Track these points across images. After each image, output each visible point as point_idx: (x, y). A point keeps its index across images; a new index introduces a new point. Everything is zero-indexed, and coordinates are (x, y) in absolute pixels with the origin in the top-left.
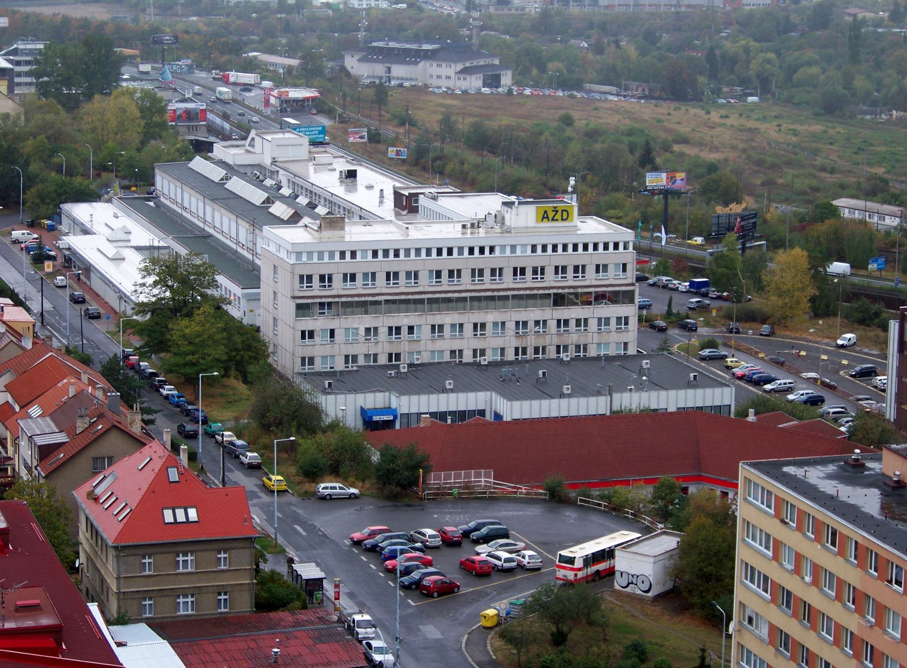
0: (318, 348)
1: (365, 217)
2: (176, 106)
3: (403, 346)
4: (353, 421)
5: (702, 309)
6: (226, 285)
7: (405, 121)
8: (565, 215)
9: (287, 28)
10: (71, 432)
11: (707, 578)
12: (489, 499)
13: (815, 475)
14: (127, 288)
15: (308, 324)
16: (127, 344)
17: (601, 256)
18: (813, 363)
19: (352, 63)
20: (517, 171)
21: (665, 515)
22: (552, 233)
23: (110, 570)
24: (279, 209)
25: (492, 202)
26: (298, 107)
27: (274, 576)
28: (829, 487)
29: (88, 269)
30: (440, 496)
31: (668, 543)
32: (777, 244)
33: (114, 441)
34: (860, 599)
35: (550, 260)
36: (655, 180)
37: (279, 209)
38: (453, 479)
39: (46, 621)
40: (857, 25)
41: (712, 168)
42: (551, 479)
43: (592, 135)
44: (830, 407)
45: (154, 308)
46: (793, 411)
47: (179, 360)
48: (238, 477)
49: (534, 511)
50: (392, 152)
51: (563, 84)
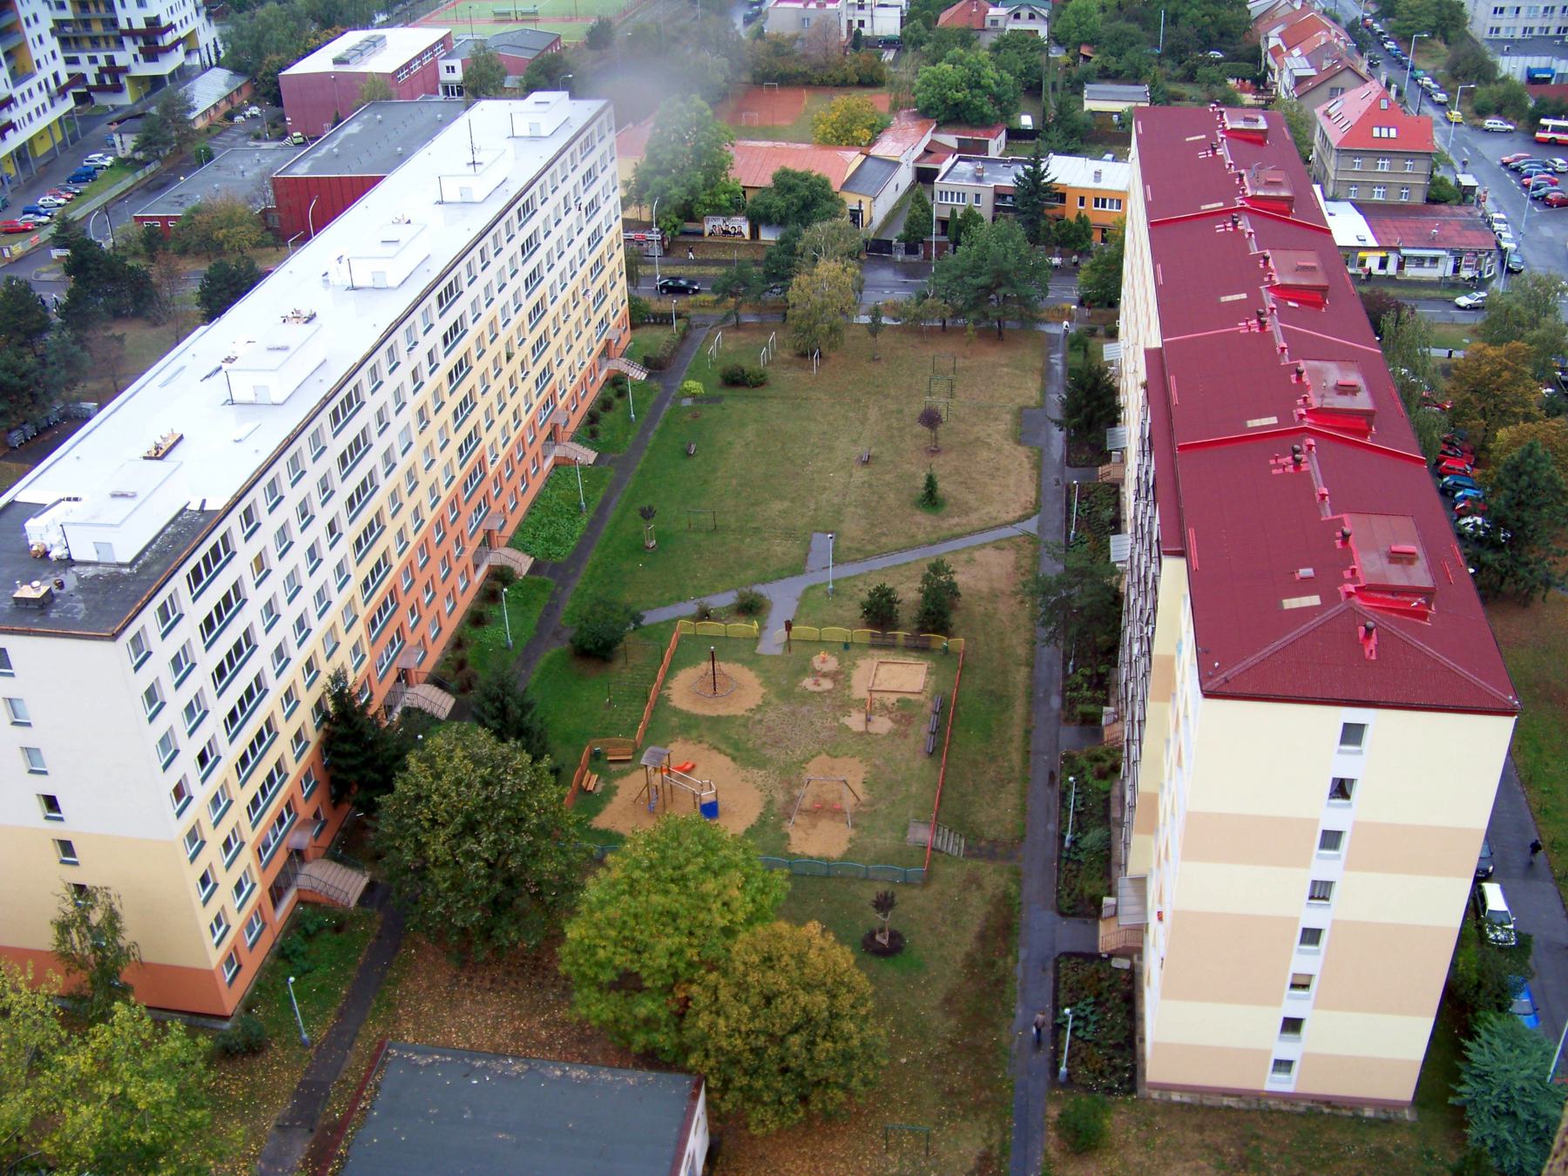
10: (1318, 69)
23: (1331, 164)
27: (1442, 182)
33: (1347, 78)
39: (1284, 193)
48: (1429, 110)
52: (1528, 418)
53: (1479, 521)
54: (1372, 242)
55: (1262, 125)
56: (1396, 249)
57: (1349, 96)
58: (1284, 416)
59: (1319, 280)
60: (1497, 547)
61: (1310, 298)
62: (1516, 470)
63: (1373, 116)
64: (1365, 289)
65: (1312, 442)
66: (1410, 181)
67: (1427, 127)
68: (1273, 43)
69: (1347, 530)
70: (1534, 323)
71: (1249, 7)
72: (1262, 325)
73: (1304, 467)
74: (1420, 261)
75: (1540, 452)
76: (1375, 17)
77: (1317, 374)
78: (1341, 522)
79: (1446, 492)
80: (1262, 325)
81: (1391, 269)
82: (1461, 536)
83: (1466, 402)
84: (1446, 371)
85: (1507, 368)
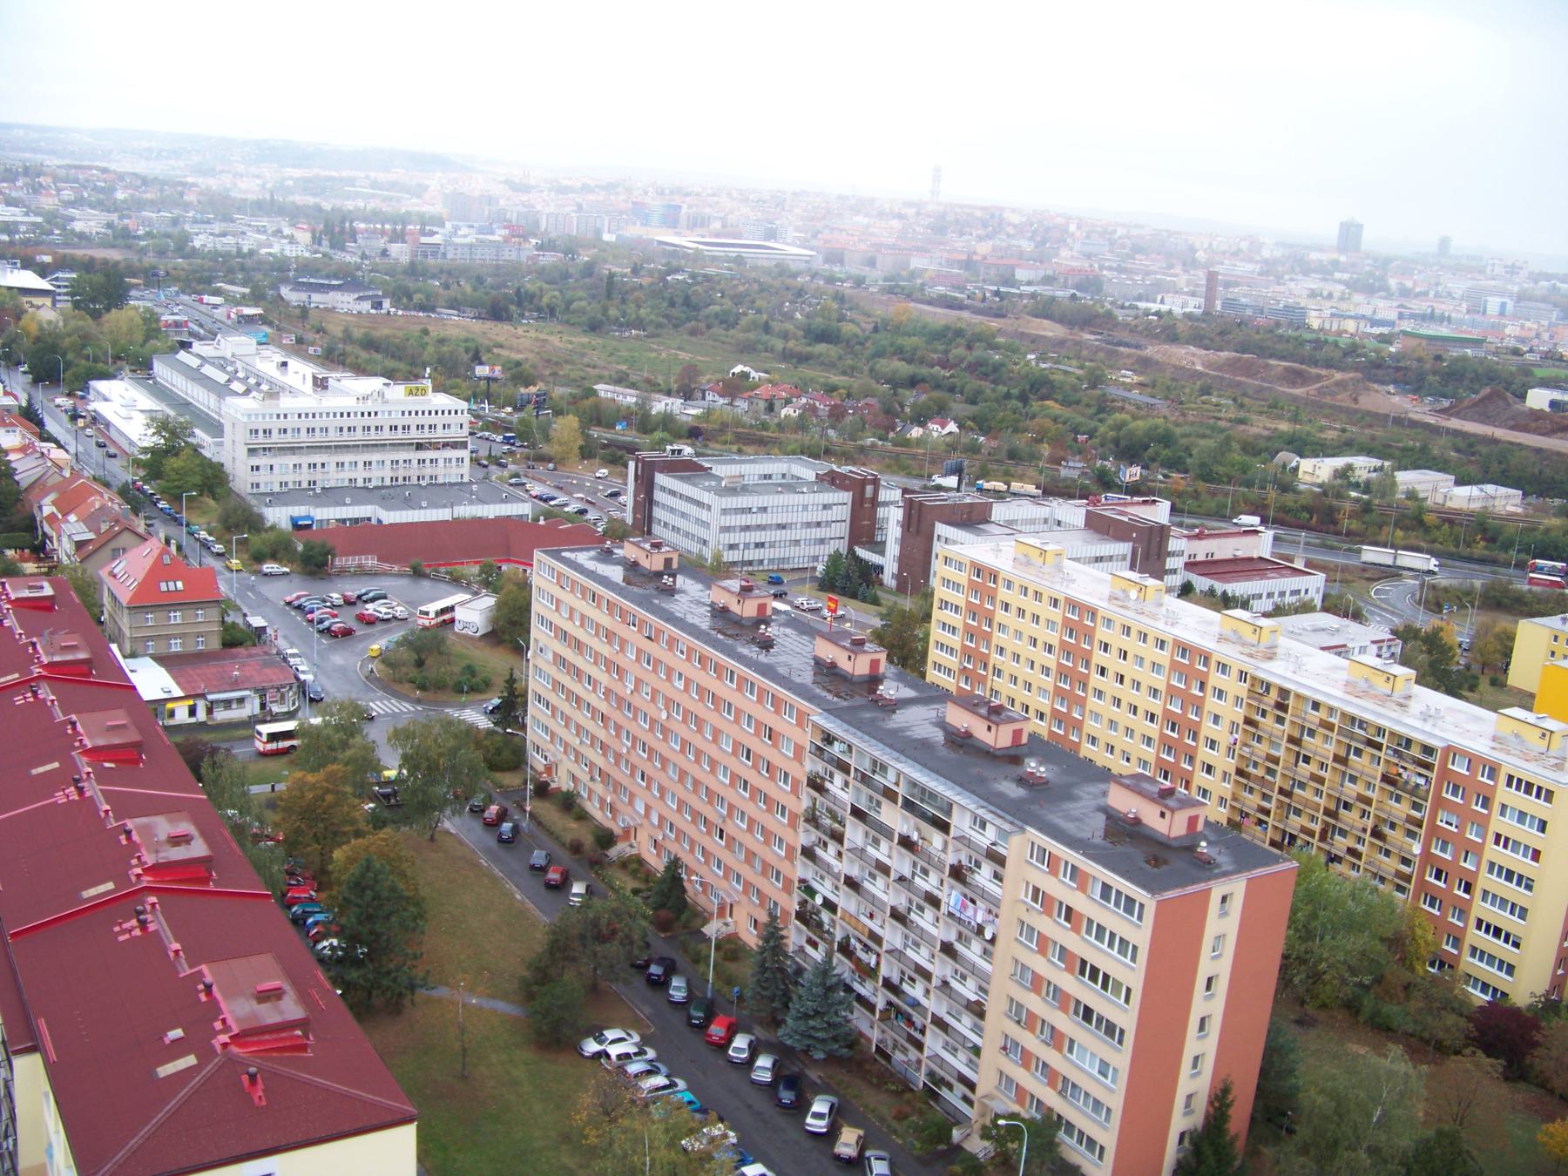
0: (263, 477)
1: (292, 392)
2: (167, 318)
3: (318, 476)
4: (286, 525)
5: (511, 453)
6: (201, 436)
7: (320, 330)
8: (424, 392)
9: (243, 269)
10: (97, 532)
11: (513, 623)
12: (375, 574)
13: (583, 558)
14: (135, 438)
15: (255, 461)
16: (135, 474)
17: (447, 419)
18: (580, 488)
19: (285, 291)
20: (391, 364)
21: (487, 584)
22: (416, 403)
23: (125, 622)
24: (237, 386)
25: (375, 383)
26: (250, 320)
28: (591, 565)
29: (108, 425)
30: (342, 573)
31: (488, 601)
32: (558, 413)
33: (126, 538)
34: (610, 635)
35: (414, 421)
36: (482, 371)
37: (237, 386)
38: (351, 562)
39: (82, 655)
40: (611, 276)
41: (518, 364)
42: (414, 561)
43: (442, 341)
44: (591, 516)
45: (153, 451)
46: (568, 518)
47: (170, 484)
48: (210, 561)
49: (404, 582)
50: (311, 350)
51: (422, 308)
52: (358, 834)
53: (335, 942)
54: (178, 692)
55: (48, 591)
56: (203, 696)
57: (130, 555)
58: (121, 878)
59: (133, 736)
60: (358, 963)
61: (126, 755)
62: (358, 886)
63: (159, 571)
64: (179, 739)
65: (153, 899)
66: (203, 629)
67: (211, 574)
68: (47, 510)
69: (209, 979)
70: (345, 745)
71: (17, 478)
72: (81, 791)
73: (152, 927)
74: (227, 704)
75: (378, 866)
76: (145, 480)
77: (147, 831)
78: (200, 973)
79: (299, 922)
80: (81, 791)
81: (201, 715)
82: (322, 960)
83: (298, 831)
84: (272, 805)
85: (328, 791)
